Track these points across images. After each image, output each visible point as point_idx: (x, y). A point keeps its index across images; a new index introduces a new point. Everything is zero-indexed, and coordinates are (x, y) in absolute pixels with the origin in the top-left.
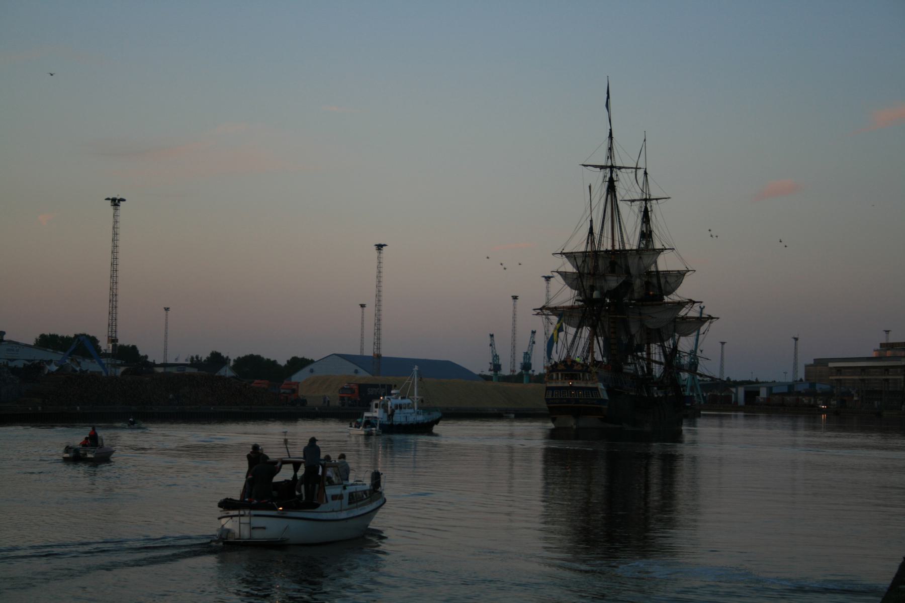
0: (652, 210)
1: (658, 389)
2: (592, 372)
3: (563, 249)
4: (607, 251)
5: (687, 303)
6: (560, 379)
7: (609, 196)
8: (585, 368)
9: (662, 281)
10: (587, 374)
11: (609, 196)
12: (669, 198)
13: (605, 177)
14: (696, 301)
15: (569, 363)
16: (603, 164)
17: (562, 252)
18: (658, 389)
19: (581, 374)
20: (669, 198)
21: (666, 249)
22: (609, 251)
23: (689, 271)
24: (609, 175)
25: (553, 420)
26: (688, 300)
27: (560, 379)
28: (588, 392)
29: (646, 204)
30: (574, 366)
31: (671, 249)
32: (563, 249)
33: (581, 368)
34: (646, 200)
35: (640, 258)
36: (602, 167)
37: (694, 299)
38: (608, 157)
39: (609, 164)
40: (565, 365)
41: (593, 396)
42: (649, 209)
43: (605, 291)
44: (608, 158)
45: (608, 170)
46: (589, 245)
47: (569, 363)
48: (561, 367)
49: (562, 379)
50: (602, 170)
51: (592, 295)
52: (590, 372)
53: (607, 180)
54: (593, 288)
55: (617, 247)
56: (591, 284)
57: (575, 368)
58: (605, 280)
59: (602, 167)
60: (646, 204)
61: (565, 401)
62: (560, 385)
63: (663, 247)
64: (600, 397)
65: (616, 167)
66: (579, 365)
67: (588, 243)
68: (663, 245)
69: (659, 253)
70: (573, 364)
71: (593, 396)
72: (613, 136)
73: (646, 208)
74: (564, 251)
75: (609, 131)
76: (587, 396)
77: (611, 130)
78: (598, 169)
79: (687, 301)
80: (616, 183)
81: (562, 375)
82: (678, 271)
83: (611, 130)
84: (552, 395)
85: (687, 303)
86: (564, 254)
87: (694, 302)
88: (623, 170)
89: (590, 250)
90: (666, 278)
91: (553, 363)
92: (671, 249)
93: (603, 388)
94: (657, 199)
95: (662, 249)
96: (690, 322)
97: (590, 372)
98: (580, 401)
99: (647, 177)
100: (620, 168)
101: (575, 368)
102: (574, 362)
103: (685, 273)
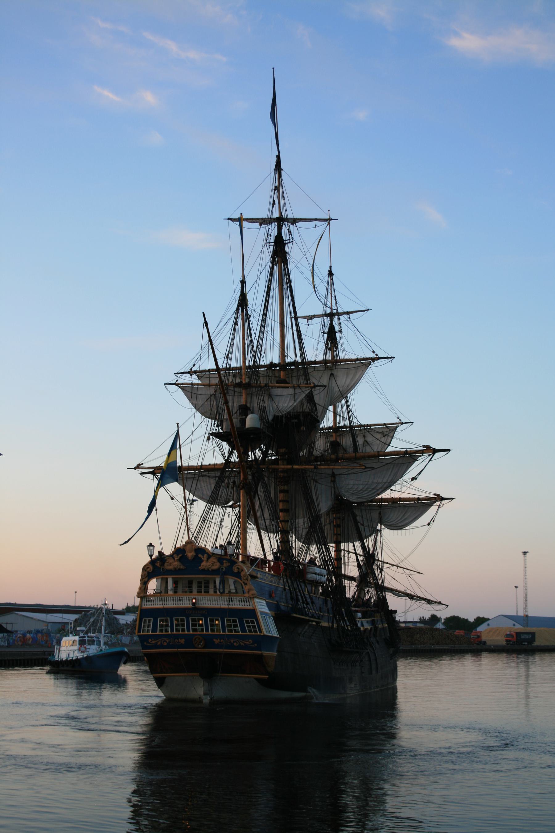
0: (340, 331)
1: (363, 617)
2: (242, 574)
3: (194, 365)
4: (272, 365)
5: (422, 452)
6: (170, 593)
7: (276, 269)
8: (226, 564)
9: (360, 441)
10: (231, 581)
11: (276, 269)
12: (369, 310)
13: (269, 235)
14: (437, 448)
15: (190, 555)
16: (264, 215)
17: (191, 369)
18: (363, 617)
19: (218, 581)
20: (369, 310)
21: (379, 358)
22: (276, 365)
23: (402, 423)
24: (275, 233)
25: (160, 683)
26: (423, 446)
27: (170, 593)
28: (235, 621)
29: (332, 320)
30: (203, 561)
31: (387, 358)
32: (194, 365)
33: (217, 566)
34: (331, 315)
35: (332, 375)
36: (263, 222)
37: (434, 446)
38: (274, 201)
39: (276, 215)
40: (180, 560)
41: (243, 630)
42: (337, 329)
43: (271, 418)
44: (274, 203)
45: (274, 226)
46: (238, 328)
47: (190, 555)
48: (175, 564)
49: (175, 592)
50: (263, 226)
51: (243, 422)
52: (238, 575)
53: (273, 240)
54: (245, 410)
55: (291, 357)
56: (243, 402)
57: (205, 565)
58: (270, 396)
59: (263, 222)
60: (332, 320)
61: (182, 641)
62: (170, 604)
63: (373, 355)
64: (261, 631)
65: (287, 220)
66: (212, 559)
67: (236, 324)
68: (373, 352)
69: (367, 365)
70: (200, 555)
71: (243, 630)
72: (283, 166)
73: (332, 327)
74: (194, 369)
75: (275, 159)
76: (161, 631)
77: (278, 157)
78: (257, 225)
79: (422, 448)
80: (288, 248)
81: (175, 582)
82: (385, 424)
83: (278, 157)
84: (154, 630)
85: (422, 452)
86: (195, 372)
87: (435, 451)
88: (299, 224)
89: (239, 364)
90: (364, 436)
91: (156, 554)
92: (387, 358)
93: (266, 610)
94: (348, 313)
95: (373, 360)
96: (405, 506)
97: (238, 575)
98: (217, 641)
99: (332, 279)
100: (294, 221)
101: (205, 565)
102: (202, 551)
103: (397, 427)
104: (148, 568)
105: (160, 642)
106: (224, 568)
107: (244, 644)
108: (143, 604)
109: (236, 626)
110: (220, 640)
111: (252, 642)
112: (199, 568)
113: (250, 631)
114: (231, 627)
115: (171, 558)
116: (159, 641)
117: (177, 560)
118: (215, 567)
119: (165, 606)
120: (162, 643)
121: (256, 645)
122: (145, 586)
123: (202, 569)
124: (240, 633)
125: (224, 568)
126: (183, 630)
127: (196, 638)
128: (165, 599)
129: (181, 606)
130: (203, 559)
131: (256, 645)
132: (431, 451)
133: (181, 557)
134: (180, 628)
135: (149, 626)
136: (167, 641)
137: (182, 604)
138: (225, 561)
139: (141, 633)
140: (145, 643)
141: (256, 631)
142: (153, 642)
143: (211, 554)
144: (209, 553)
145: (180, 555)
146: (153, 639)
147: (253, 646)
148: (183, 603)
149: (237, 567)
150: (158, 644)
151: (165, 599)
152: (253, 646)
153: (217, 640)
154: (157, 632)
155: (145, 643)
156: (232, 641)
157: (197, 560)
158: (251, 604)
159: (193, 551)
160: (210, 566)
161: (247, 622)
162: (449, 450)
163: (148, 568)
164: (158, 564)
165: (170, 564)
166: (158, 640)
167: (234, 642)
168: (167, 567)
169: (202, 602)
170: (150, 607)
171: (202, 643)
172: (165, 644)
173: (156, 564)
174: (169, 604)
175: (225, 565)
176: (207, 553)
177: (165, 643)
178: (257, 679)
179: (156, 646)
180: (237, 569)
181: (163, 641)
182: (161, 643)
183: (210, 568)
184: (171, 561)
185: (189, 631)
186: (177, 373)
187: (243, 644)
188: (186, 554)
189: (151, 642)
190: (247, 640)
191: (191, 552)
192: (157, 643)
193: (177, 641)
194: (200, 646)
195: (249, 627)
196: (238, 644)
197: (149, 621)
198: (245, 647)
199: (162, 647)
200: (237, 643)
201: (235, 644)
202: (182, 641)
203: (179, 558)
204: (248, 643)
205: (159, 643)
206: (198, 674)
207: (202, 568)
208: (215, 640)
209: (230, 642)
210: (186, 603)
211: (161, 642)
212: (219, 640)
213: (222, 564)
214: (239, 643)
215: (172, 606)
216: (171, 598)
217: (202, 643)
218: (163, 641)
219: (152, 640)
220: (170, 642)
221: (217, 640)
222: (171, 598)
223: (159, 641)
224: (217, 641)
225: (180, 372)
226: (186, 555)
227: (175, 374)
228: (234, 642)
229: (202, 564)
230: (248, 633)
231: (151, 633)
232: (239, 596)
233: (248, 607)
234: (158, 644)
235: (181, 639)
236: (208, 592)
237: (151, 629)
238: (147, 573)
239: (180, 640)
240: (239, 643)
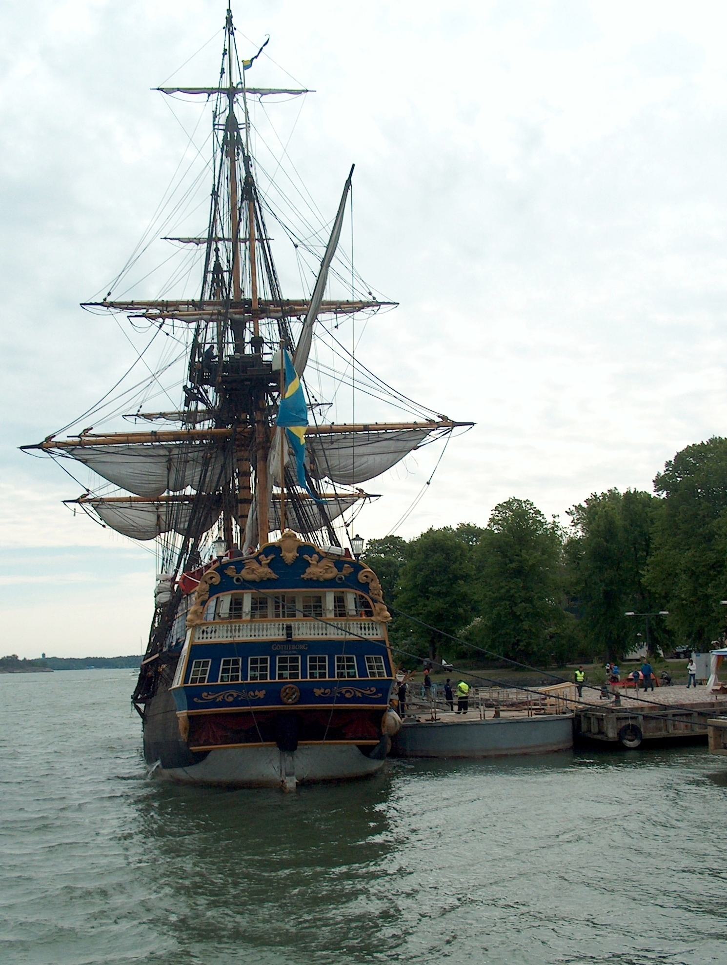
3: (109, 294)
8: (347, 570)
15: (289, 556)
17: (105, 300)
27: (246, 617)
28: (350, 660)
30: (308, 564)
32: (109, 294)
33: (333, 573)
37: (453, 417)
41: (363, 673)
47: (289, 556)
49: (252, 616)
57: (315, 571)
61: (261, 694)
62: (245, 634)
66: (324, 562)
71: (363, 673)
84: (213, 677)
98: (318, 692)
104: (211, 578)
105: (222, 697)
106: (343, 577)
107: (363, 694)
108: (197, 637)
109: (352, 667)
110: (325, 690)
111: (374, 691)
112: (302, 576)
113: (373, 674)
114: (343, 668)
115: (254, 561)
116: (221, 695)
117: (266, 564)
118: (329, 576)
119: (237, 639)
120: (226, 699)
121: (380, 695)
122: (202, 607)
123: (307, 579)
124: (357, 678)
125: (343, 577)
126: (265, 677)
127: (286, 689)
128: (237, 628)
129: (265, 638)
130: (310, 561)
131: (380, 695)
132: (448, 424)
133: (272, 559)
134: (286, 673)
135: (204, 672)
136: (235, 695)
137: (326, 634)
138: (346, 565)
139: (189, 684)
140: (195, 700)
141: (380, 674)
142: (210, 697)
143: (324, 555)
144: (321, 553)
145: (270, 558)
146: (210, 693)
147: (374, 697)
148: (269, 634)
149: (365, 574)
150: (218, 700)
151: (237, 628)
152: (374, 697)
153: (320, 689)
154: (217, 682)
155: (195, 700)
156: (344, 691)
157: (301, 564)
158: (379, 632)
159: (295, 551)
160: (321, 574)
161: (369, 660)
162: (473, 424)
163: (211, 578)
164: (231, 572)
165: (253, 570)
166: (217, 695)
167: (346, 692)
168: (245, 574)
169: (300, 632)
170: (209, 641)
171: (294, 696)
172: (231, 699)
173: (226, 572)
174: (243, 636)
175: (344, 572)
176: (318, 553)
177: (229, 697)
178: (360, 747)
179: (214, 704)
180: (365, 578)
181: (226, 696)
182: (223, 700)
183: (321, 576)
184: (255, 565)
185: (273, 677)
186: (85, 304)
187: (361, 696)
188: (281, 555)
189: (207, 696)
190: (368, 688)
191: (290, 552)
192: (215, 698)
193: (252, 694)
194: (290, 700)
195: (371, 667)
196: (352, 695)
197: (205, 664)
198: (365, 699)
199: (224, 704)
200: (351, 693)
201: (348, 695)
202: (261, 694)
203: (268, 561)
204: (368, 692)
205: (220, 699)
206: (274, 743)
207: (308, 577)
208: (315, 690)
209: (340, 693)
210: (272, 632)
211: (224, 697)
212: (322, 690)
213: (340, 570)
214: (355, 692)
215: (249, 639)
216: (247, 626)
217: (294, 696)
218: (226, 696)
219: (208, 694)
220: (238, 696)
221: (320, 689)
222: (247, 626)
223: (221, 695)
224: (318, 692)
225: (89, 302)
226: (282, 557)
227: (81, 304)
228: (346, 692)
229: (308, 570)
230: (370, 678)
231: (206, 683)
232: (311, 620)
233: (375, 637)
234: (218, 700)
235: (259, 691)
236: (265, 616)
237: (207, 676)
238: (208, 586)
239: (257, 693)
240: (355, 692)
